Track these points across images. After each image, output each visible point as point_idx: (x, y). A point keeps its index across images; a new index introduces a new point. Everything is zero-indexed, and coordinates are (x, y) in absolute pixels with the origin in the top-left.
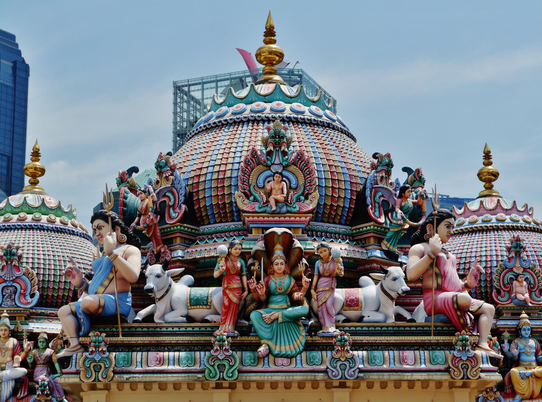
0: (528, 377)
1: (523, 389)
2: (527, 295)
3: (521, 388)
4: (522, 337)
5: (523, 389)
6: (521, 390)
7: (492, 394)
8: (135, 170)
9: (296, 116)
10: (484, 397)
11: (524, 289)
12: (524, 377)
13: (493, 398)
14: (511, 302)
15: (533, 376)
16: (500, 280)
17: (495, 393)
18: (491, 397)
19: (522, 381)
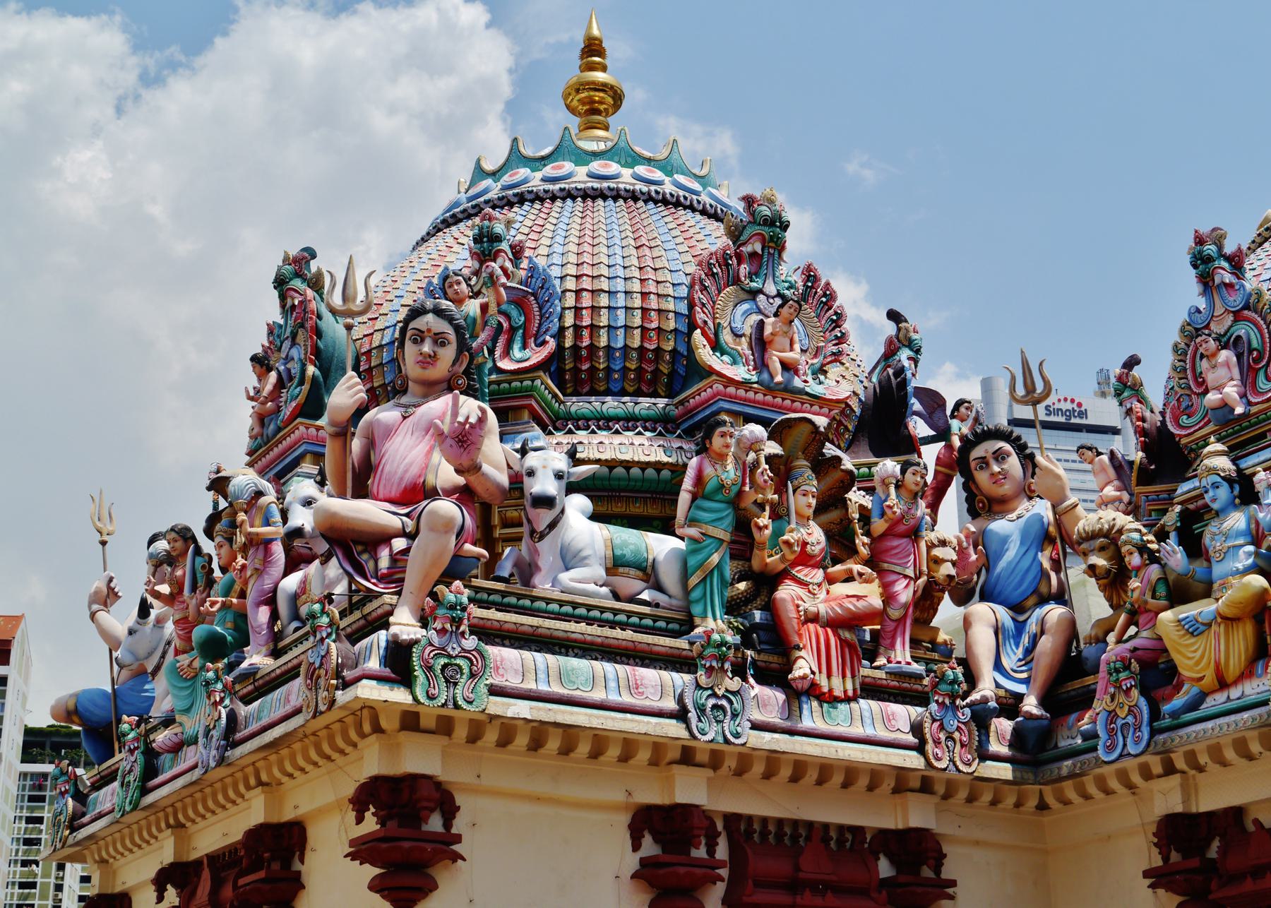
0: (1209, 625)
1: (1198, 663)
2: (1231, 391)
3: (1191, 663)
4: (1217, 514)
5: (1198, 663)
6: (1190, 669)
7: (1122, 698)
8: (1132, 362)
9: (645, 189)
10: (1110, 712)
11: (1222, 373)
12: (1194, 629)
13: (1126, 708)
14: (1209, 422)
15: (1219, 620)
16: (1185, 370)
17: (1127, 692)
18: (1121, 705)
19: (1193, 640)
